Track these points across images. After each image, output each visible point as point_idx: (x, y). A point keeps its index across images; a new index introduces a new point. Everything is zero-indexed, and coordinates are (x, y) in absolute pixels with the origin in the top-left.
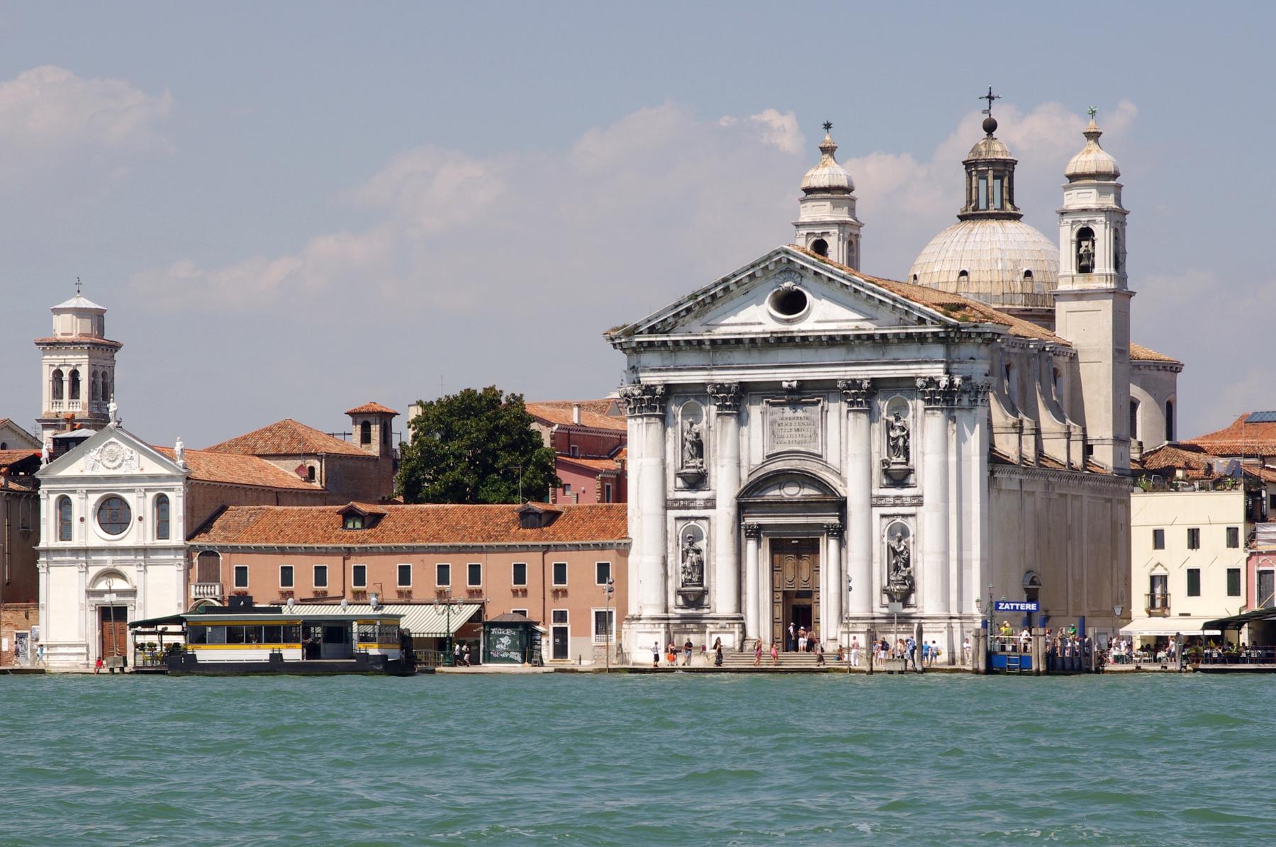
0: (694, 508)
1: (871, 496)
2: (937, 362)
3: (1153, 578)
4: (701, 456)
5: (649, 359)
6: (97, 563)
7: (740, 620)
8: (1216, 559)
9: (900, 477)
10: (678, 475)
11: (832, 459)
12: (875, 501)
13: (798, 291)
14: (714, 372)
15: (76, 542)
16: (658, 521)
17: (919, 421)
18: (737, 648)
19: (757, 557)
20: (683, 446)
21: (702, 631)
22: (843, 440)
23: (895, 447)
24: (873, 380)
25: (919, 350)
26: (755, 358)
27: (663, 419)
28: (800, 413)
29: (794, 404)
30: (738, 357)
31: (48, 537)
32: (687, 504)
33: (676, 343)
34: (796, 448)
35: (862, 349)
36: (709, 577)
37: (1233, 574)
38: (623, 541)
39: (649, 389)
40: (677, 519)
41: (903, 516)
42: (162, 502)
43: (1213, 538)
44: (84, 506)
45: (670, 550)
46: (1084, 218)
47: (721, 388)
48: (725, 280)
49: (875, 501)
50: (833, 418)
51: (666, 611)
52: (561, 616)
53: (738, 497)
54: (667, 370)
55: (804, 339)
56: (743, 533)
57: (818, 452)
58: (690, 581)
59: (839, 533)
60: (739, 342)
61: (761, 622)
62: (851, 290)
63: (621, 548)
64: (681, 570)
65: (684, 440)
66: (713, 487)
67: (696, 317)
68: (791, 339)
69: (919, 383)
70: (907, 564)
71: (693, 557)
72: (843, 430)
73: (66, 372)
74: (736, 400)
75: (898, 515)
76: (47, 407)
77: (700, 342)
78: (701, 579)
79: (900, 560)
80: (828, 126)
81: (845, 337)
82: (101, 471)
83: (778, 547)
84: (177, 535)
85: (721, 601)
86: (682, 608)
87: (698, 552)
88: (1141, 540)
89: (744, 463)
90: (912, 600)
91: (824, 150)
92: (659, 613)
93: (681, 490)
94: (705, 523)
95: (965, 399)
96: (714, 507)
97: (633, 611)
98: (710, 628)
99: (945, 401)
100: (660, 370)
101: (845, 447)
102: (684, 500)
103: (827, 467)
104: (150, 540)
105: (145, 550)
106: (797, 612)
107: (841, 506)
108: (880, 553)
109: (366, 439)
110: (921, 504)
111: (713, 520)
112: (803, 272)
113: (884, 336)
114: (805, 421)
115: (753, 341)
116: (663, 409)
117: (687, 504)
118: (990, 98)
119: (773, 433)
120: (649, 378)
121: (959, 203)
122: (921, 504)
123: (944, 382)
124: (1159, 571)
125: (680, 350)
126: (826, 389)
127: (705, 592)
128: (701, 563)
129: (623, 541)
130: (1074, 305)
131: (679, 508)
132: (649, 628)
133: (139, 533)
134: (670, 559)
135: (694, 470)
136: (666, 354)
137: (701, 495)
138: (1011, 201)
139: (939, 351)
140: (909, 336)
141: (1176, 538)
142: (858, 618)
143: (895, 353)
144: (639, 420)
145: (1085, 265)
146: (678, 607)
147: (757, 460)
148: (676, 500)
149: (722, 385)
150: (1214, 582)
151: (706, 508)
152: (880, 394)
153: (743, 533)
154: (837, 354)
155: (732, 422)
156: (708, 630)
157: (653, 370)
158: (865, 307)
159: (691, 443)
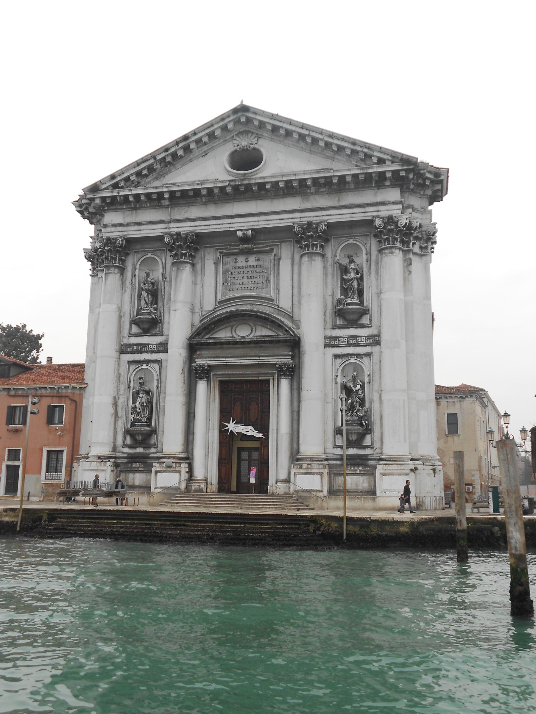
0: (147, 352)
1: (326, 338)
2: (394, 203)
4: (156, 304)
5: (111, 217)
7: (188, 458)
9: (354, 317)
10: (134, 322)
11: (285, 303)
12: (330, 342)
13: (254, 149)
14: (172, 225)
16: (111, 363)
17: (373, 264)
18: (183, 486)
20: (140, 296)
21: (148, 470)
22: (296, 284)
23: (351, 288)
24: (330, 225)
25: (375, 195)
26: (212, 211)
27: (122, 270)
28: (252, 260)
29: (247, 253)
30: (195, 212)
32: (140, 349)
33: (137, 197)
34: (248, 294)
35: (317, 197)
36: (158, 418)
38: (78, 386)
40: (130, 362)
41: (358, 356)
45: (122, 392)
48: (186, 138)
50: (285, 266)
51: (114, 449)
53: (191, 338)
54: (128, 224)
55: (261, 186)
56: (193, 376)
57: (272, 295)
58: (139, 421)
59: (293, 372)
60: (197, 193)
61: (206, 464)
62: (309, 140)
63: (77, 391)
64: (130, 410)
65: (141, 290)
66: (165, 332)
67: (157, 178)
68: (248, 187)
69: (378, 222)
70: (362, 404)
72: (296, 276)
74: (188, 248)
75: (352, 355)
77: (160, 195)
78: (150, 419)
81: (302, 182)
86: (130, 447)
87: (148, 393)
89: (197, 310)
90: (367, 441)
92: (106, 450)
93: (136, 335)
94: (156, 366)
96: (166, 351)
97: (83, 451)
98: (156, 466)
99: (403, 242)
100: (121, 225)
102: (138, 345)
103: (279, 310)
107: (295, 344)
110: (378, 343)
111: (164, 363)
112: (260, 132)
113: (342, 178)
114: (258, 269)
115: (210, 190)
116: (123, 261)
117: (140, 349)
119: (225, 281)
122: (378, 343)
125: (140, 208)
127: (154, 432)
128: (150, 403)
129: (78, 386)
131: (133, 352)
132: (94, 466)
134: (122, 400)
135: (148, 316)
136: (128, 213)
137: (153, 340)
139: (394, 194)
140: (369, 176)
142: (311, 459)
144: (100, 274)
146: (125, 446)
147: (209, 306)
148: (130, 345)
149: (178, 234)
151: (158, 352)
152: (334, 242)
153: (194, 374)
155: (187, 270)
156: (153, 470)
157: (114, 225)
159: (147, 291)
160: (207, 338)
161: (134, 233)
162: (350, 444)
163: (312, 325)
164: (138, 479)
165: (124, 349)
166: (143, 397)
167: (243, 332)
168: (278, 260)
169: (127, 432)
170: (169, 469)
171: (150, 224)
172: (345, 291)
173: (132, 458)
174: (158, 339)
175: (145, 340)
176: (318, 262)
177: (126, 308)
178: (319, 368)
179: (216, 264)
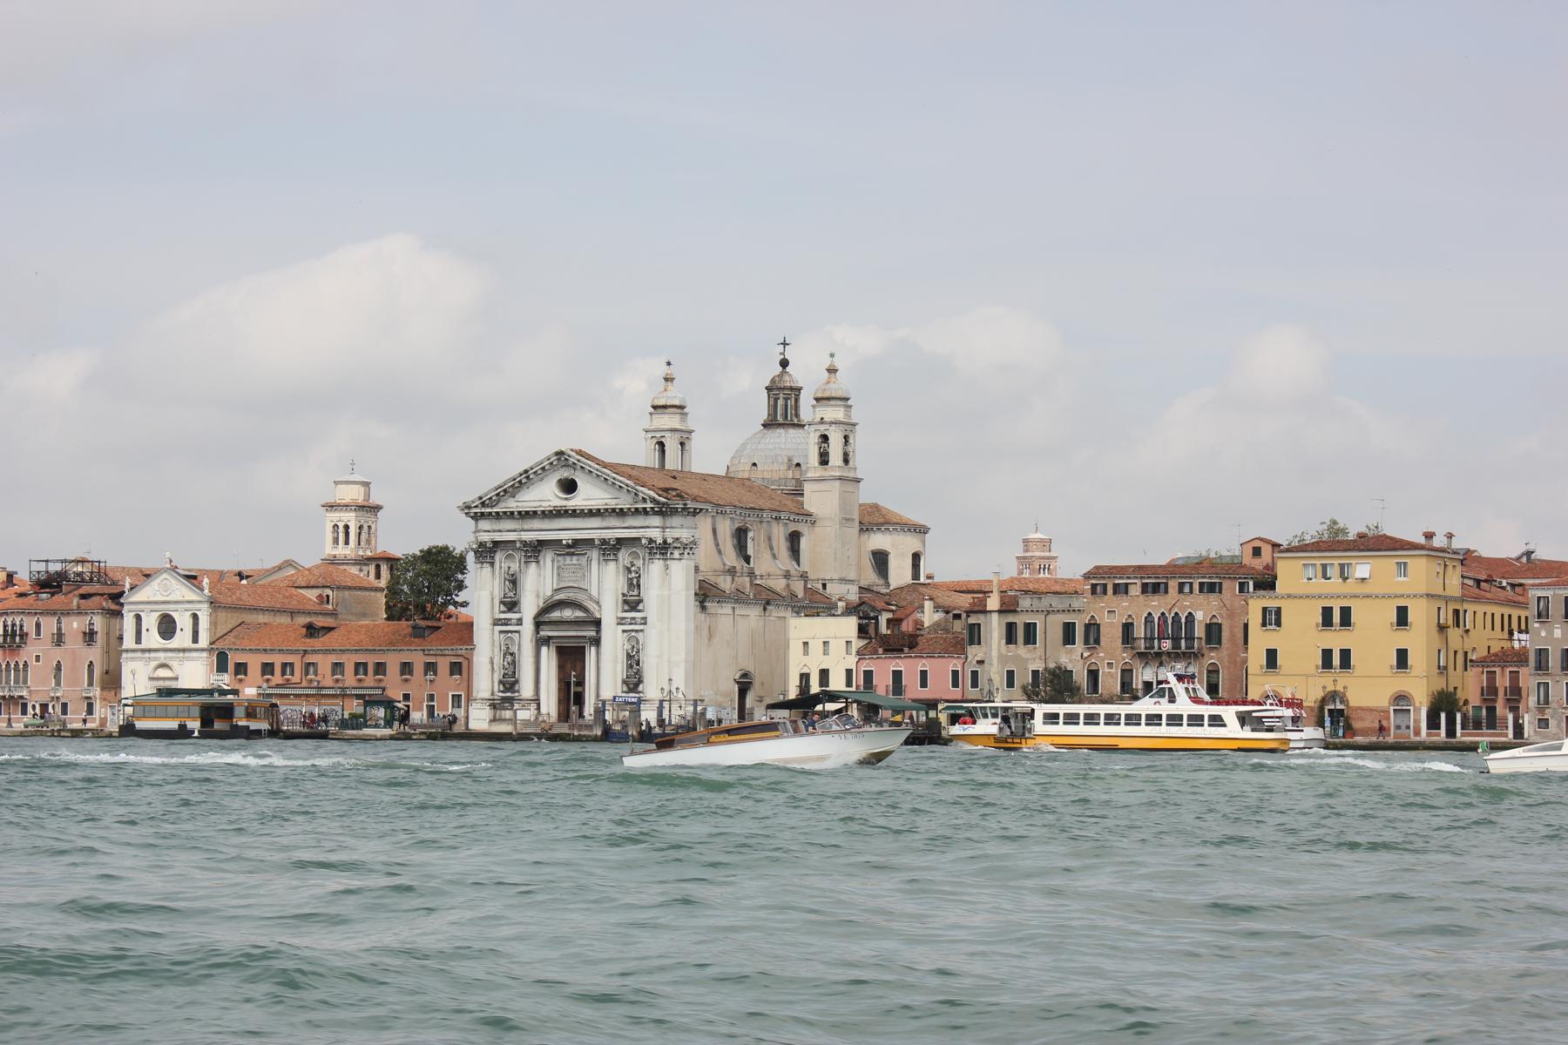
3: (802, 675)
5: (485, 525)
6: (155, 659)
7: (537, 701)
11: (594, 593)
12: (621, 621)
15: (143, 646)
19: (549, 658)
24: (618, 540)
26: (546, 524)
27: (492, 564)
30: (536, 524)
31: (129, 641)
32: (506, 622)
37: (849, 672)
39: (481, 545)
42: (195, 617)
43: (837, 647)
44: (151, 621)
46: (822, 427)
47: (525, 543)
48: (526, 471)
49: (621, 621)
50: (594, 564)
52: (431, 698)
59: (596, 642)
61: (550, 704)
71: (509, 658)
73: (341, 525)
76: (329, 550)
79: (633, 661)
80: (669, 364)
83: (562, 652)
84: (204, 641)
85: (526, 690)
88: (795, 649)
90: (640, 688)
92: (487, 695)
95: (676, 554)
101: (604, 584)
103: (591, 599)
104: (188, 643)
106: (571, 695)
108: (622, 657)
109: (378, 576)
117: (506, 622)
118: (785, 344)
121: (764, 415)
123: (659, 541)
124: (805, 670)
126: (589, 542)
127: (517, 682)
128: (514, 662)
130: (816, 486)
133: (182, 638)
134: (496, 660)
138: (797, 415)
139: (656, 521)
141: (816, 647)
143: (630, 521)
145: (824, 459)
147: (549, 593)
153: (541, 642)
158: (611, 490)
160: (546, 618)
161: (498, 537)
162: (630, 690)
163: (609, 612)
164: (508, 714)
165: (496, 622)
166: (509, 658)
167: (568, 614)
168: (589, 561)
169: (501, 682)
170: (523, 708)
171: (507, 532)
172: (630, 585)
173: (504, 699)
174: (517, 616)
176: (612, 565)
177: (496, 592)
178: (613, 641)
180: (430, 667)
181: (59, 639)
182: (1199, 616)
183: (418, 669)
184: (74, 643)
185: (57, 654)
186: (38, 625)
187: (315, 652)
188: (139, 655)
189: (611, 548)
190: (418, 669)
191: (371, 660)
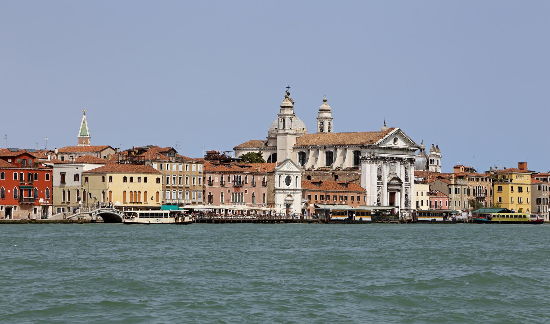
8: (426, 198)
15: (282, 187)
30: (388, 152)
43: (425, 194)
44: (283, 178)
82: (288, 170)
84: (299, 187)
91: (324, 101)
104: (295, 188)
105: (294, 190)
120: (376, 155)
133: (292, 185)
141: (420, 193)
150: (425, 203)
153: (388, 190)
154: (401, 152)
175: (379, 181)
179: (389, 164)
180: (359, 198)
181: (254, 185)
182: (484, 187)
183: (355, 198)
184: (259, 185)
185: (253, 190)
186: (246, 178)
187: (329, 192)
188: (281, 191)
189: (401, 160)
190: (355, 198)
191: (344, 195)
